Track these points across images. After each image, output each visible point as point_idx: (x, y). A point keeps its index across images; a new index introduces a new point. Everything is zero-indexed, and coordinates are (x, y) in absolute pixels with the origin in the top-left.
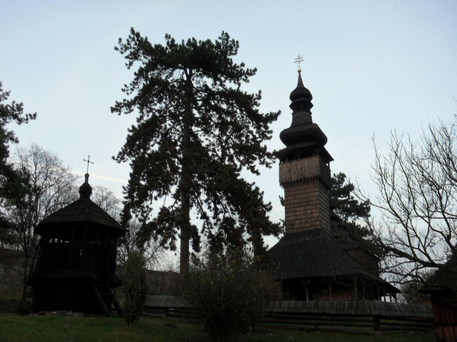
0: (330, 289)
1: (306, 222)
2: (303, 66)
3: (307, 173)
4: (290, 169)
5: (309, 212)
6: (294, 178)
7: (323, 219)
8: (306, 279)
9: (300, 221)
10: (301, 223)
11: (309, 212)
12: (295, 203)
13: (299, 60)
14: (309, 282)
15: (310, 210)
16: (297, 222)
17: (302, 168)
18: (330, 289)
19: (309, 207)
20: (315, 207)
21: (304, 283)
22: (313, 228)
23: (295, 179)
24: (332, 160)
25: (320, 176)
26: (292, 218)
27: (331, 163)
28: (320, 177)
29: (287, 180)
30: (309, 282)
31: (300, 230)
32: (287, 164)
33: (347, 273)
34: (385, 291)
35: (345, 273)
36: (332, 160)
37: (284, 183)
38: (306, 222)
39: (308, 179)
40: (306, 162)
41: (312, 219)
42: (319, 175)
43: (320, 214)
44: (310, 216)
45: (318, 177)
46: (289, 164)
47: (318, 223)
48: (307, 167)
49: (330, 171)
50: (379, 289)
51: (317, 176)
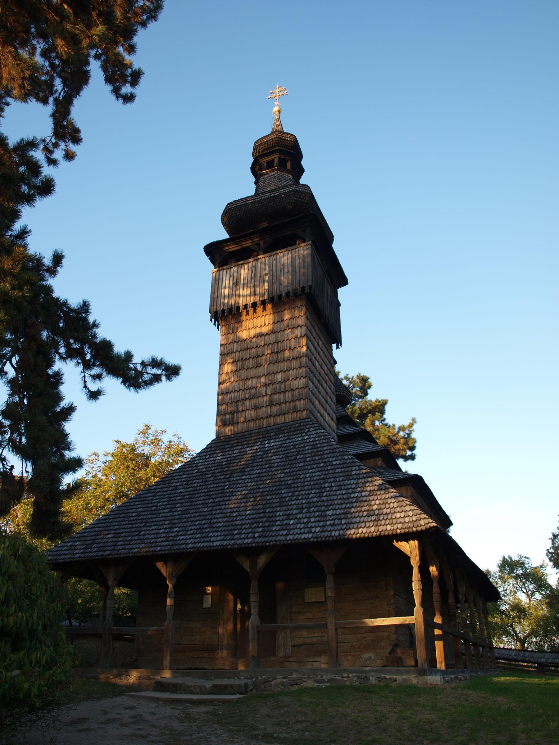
0: (330, 582)
1: (271, 404)
4: (237, 279)
5: (279, 377)
7: (318, 400)
8: (252, 552)
9: (253, 402)
10: (256, 408)
11: (279, 377)
12: (246, 359)
14: (262, 560)
15: (283, 373)
16: (248, 403)
18: (330, 582)
20: (295, 364)
21: (246, 565)
22: (288, 418)
24: (344, 281)
25: (310, 286)
28: (310, 289)
30: (262, 560)
31: (252, 425)
32: (232, 270)
33: (389, 527)
35: (381, 528)
36: (344, 281)
37: (220, 314)
38: (271, 404)
39: (280, 296)
41: (288, 394)
42: (309, 284)
43: (307, 381)
44: (283, 386)
45: (307, 290)
46: (236, 268)
47: (301, 404)
49: (339, 305)
51: (303, 289)
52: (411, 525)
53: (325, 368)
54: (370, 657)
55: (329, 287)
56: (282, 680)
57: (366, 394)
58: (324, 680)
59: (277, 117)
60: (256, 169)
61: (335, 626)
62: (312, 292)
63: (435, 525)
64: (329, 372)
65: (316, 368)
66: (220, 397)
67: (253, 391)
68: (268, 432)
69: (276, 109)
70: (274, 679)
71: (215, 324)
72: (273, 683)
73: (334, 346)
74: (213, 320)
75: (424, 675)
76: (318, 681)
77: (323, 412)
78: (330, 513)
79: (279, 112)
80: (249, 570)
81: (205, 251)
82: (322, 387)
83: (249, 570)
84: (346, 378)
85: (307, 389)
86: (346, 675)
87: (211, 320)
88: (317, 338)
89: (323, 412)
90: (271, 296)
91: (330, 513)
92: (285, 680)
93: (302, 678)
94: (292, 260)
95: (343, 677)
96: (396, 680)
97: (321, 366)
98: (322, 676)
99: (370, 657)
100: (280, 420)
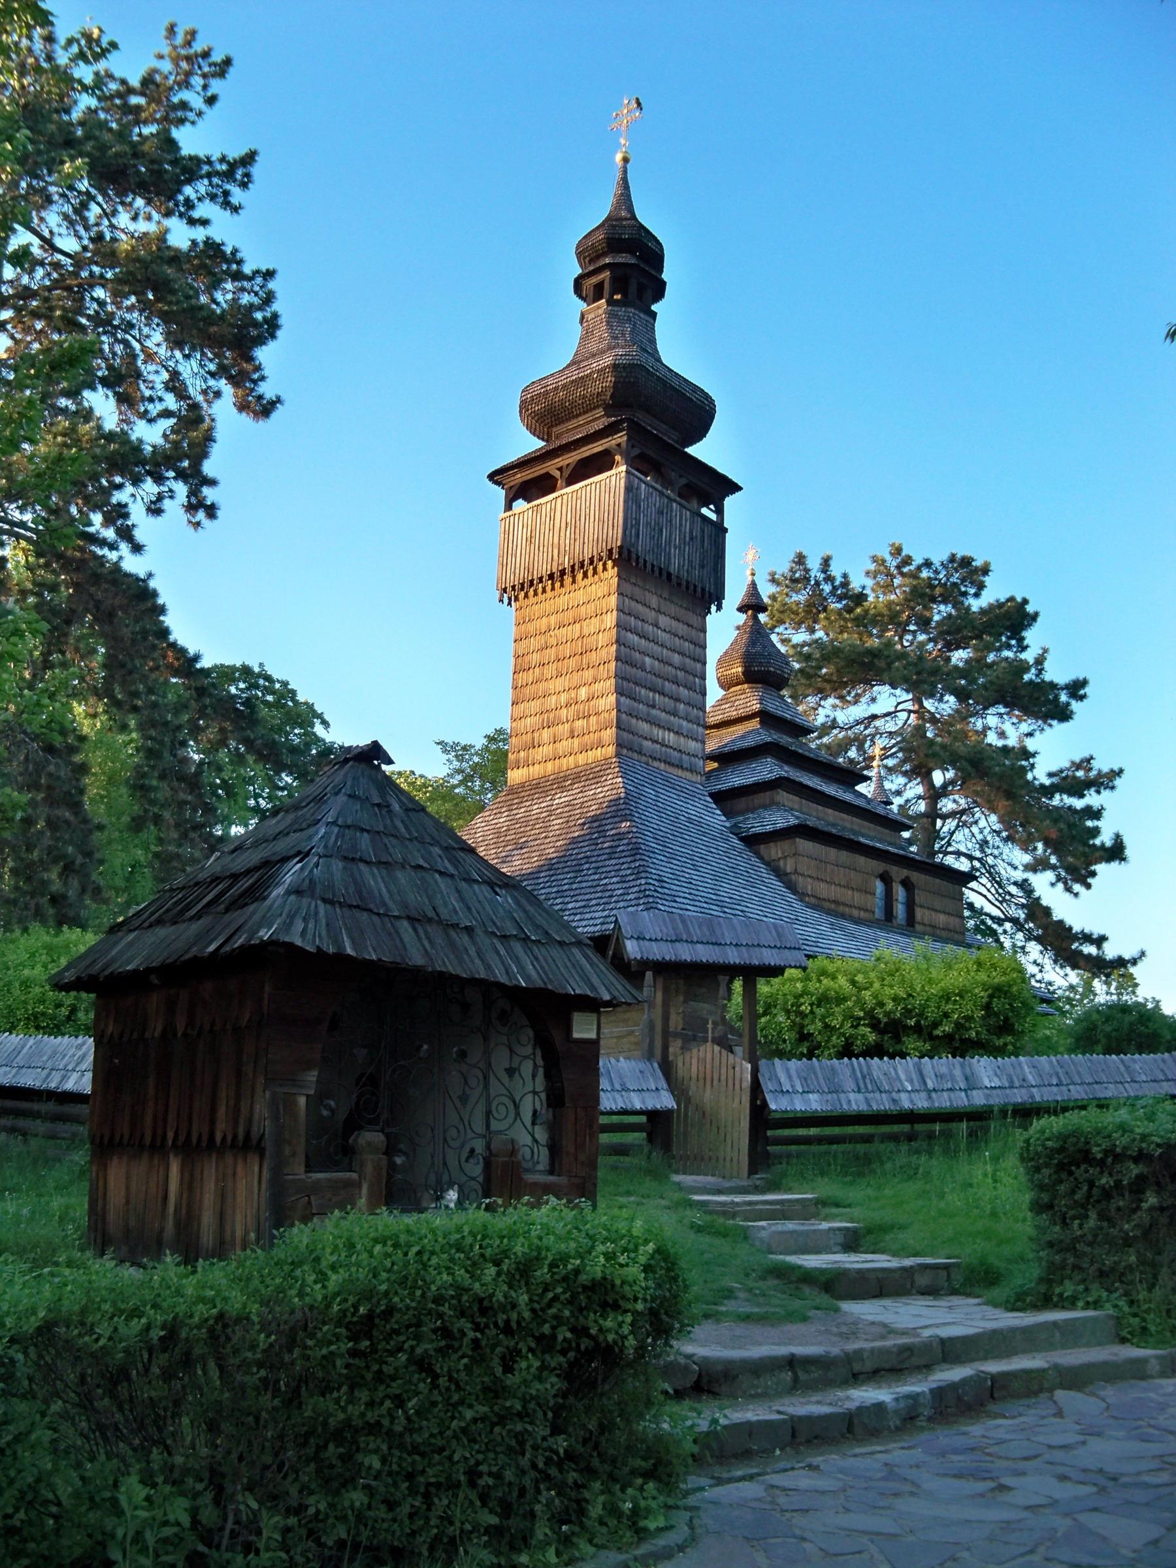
5: (583, 693)
11: (583, 693)
16: (546, 734)
19: (588, 675)
24: (733, 488)
25: (621, 547)
27: (730, 502)
36: (733, 488)
41: (593, 719)
49: (726, 530)
53: (676, 659)
57: (981, 586)
59: (618, 175)
64: (688, 660)
65: (643, 670)
68: (565, 778)
69: (619, 157)
73: (713, 608)
77: (659, 734)
78: (570, 906)
79: (626, 160)
82: (662, 693)
84: (928, 564)
87: (501, 601)
88: (651, 615)
89: (659, 734)
91: (570, 906)
94: (597, 504)
97: (661, 661)
100: (581, 759)
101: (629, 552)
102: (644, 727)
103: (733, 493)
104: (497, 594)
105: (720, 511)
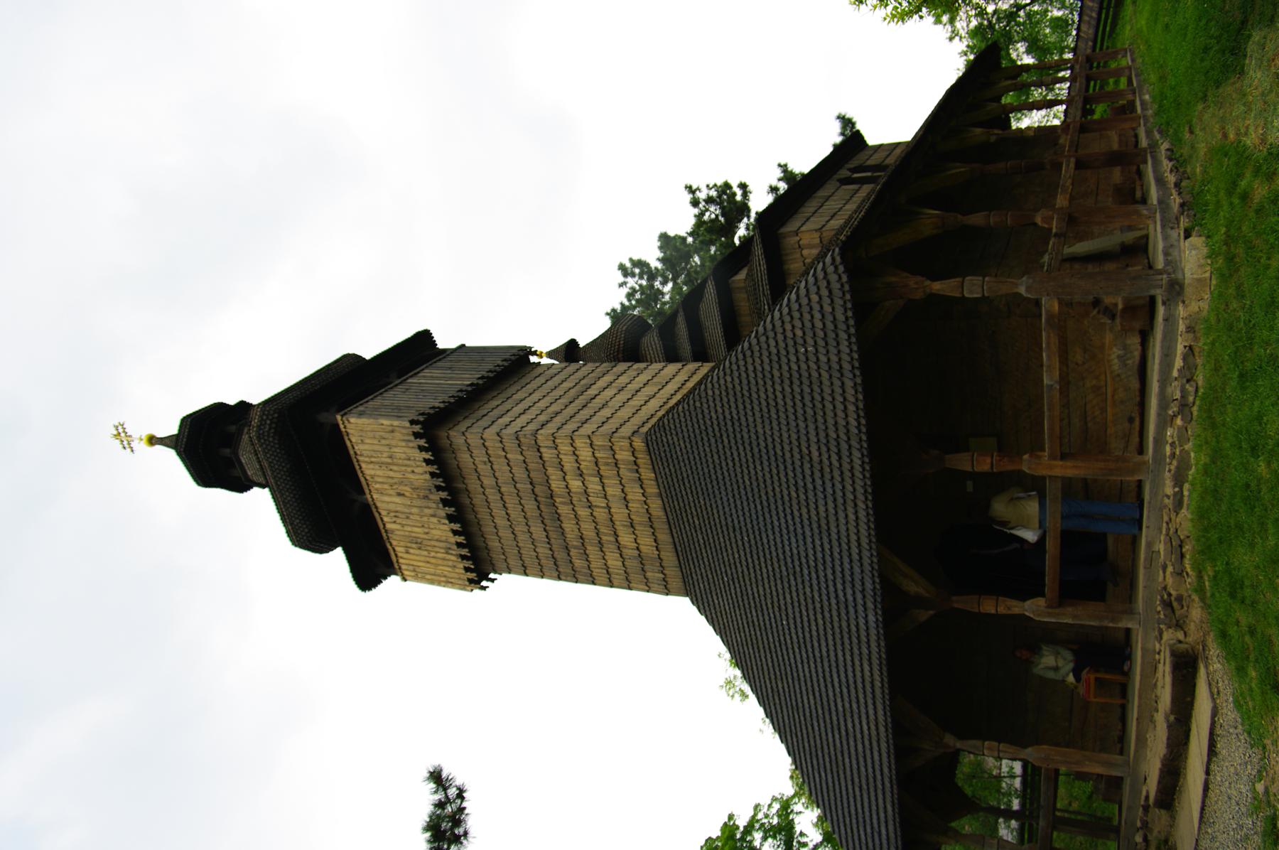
2: (138, 430)
3: (411, 476)
5: (575, 484)
6: (442, 530)
11: (575, 484)
13: (122, 435)
16: (626, 539)
17: (399, 494)
21: (924, 615)
23: (446, 527)
24: (423, 339)
25: (412, 422)
26: (614, 562)
29: (453, 558)
30: (914, 586)
34: (995, 105)
36: (423, 339)
37: (472, 576)
40: (372, 472)
42: (408, 424)
45: (417, 428)
48: (391, 474)
50: (978, 131)
52: (838, 302)
54: (1119, 357)
55: (427, 373)
56: (1168, 573)
58: (1175, 494)
60: (241, 486)
61: (1055, 459)
62: (421, 419)
63: (837, 250)
66: (615, 582)
67: (603, 530)
70: (1165, 588)
71: (493, 580)
72: (1173, 593)
74: (484, 583)
75: (1182, 286)
76: (1179, 504)
80: (931, 612)
81: (370, 589)
83: (931, 612)
85: (594, 439)
86: (1168, 448)
87: (484, 588)
90: (434, 490)
92: (1170, 569)
93: (1167, 534)
95: (1173, 455)
96: (1190, 347)
98: (1168, 497)
99: (1119, 357)
101: (422, 414)
102: (625, 413)
103: (434, 344)
104: (477, 592)
105: (444, 351)
